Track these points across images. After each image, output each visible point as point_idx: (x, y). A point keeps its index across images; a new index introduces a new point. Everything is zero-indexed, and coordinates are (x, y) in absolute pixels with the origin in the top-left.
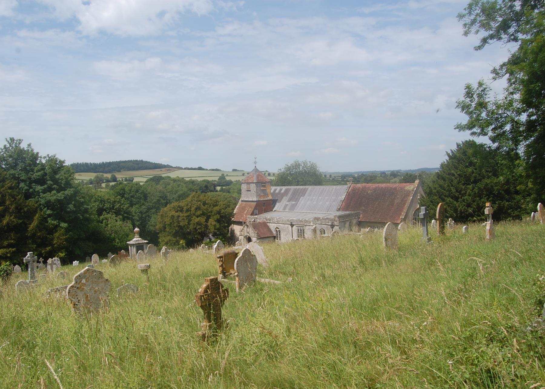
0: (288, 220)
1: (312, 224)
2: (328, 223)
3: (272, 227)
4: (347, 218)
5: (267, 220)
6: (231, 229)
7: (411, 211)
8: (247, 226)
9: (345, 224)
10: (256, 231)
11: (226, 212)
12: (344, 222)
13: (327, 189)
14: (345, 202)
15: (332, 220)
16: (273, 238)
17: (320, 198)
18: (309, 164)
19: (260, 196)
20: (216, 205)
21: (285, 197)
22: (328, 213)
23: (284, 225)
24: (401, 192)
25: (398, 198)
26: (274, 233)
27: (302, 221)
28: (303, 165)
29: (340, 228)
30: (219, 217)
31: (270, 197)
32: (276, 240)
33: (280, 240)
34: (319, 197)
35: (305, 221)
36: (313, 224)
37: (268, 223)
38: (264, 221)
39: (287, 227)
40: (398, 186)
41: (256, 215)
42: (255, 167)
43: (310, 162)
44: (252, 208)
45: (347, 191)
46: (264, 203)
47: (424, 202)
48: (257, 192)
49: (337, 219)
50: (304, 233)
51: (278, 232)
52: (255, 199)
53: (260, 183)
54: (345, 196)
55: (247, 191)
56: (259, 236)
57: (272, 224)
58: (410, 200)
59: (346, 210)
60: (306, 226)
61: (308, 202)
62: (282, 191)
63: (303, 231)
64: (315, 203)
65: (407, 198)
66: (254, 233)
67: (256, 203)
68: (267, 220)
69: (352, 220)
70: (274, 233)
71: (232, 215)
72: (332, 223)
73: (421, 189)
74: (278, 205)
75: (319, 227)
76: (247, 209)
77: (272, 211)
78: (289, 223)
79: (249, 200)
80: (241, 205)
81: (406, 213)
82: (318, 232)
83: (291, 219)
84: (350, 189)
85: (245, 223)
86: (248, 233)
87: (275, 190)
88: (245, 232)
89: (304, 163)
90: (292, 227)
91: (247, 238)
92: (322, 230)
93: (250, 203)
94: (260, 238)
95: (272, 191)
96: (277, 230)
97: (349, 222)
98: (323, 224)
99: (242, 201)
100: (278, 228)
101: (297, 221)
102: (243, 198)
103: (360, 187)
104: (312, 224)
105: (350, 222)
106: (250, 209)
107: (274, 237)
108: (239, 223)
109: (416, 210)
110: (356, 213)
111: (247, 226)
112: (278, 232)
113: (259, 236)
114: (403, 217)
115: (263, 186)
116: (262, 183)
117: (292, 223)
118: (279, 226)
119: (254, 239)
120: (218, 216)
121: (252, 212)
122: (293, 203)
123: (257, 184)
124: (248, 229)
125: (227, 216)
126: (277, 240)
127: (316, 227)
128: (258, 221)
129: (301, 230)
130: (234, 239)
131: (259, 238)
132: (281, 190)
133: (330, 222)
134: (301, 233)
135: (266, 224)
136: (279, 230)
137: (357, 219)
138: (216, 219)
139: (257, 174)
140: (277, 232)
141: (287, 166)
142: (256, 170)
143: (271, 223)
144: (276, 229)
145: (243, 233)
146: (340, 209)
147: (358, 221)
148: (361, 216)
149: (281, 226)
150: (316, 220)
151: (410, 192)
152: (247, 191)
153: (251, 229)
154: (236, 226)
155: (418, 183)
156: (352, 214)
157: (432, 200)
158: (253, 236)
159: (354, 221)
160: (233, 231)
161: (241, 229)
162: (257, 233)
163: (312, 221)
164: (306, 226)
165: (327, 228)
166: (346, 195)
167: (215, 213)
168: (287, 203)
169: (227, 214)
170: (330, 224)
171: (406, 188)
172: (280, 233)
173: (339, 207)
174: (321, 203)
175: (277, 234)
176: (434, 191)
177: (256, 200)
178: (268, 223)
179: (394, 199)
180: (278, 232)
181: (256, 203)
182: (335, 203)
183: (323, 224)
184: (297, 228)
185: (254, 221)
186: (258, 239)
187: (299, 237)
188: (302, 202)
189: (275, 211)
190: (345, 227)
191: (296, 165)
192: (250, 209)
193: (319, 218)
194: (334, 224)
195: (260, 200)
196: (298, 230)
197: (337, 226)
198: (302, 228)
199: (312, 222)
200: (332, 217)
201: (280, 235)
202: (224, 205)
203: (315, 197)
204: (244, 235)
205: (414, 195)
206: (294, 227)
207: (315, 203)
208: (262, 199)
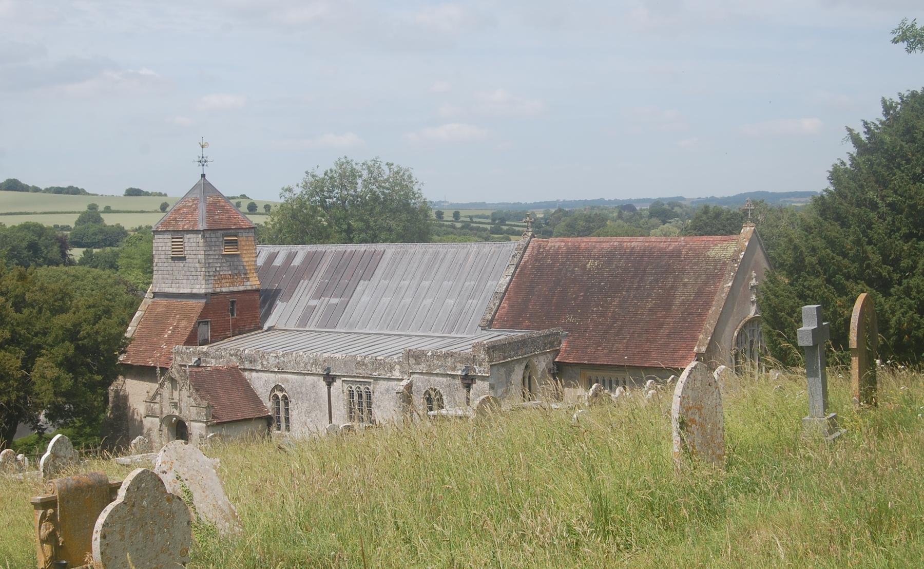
0: (315, 362)
1: (397, 374)
2: (454, 369)
3: (261, 383)
4: (516, 354)
5: (241, 360)
6: (117, 392)
7: (728, 329)
8: (173, 381)
9: (509, 374)
10: (202, 398)
11: (97, 333)
12: (508, 367)
13: (449, 256)
14: (509, 299)
15: (467, 359)
16: (265, 424)
17: (426, 284)
18: (387, 172)
19: (220, 279)
20: (63, 310)
21: (304, 283)
22: (453, 335)
24: (696, 264)
25: (685, 285)
26: (269, 404)
27: (363, 364)
28: (365, 174)
29: (492, 387)
30: (71, 351)
31: (254, 283)
32: (275, 431)
33: (288, 428)
34: (422, 280)
35: (373, 363)
36: (402, 372)
37: (245, 370)
38: (231, 365)
39: (314, 386)
40: (684, 246)
41: (205, 342)
42: (203, 176)
43: (389, 165)
44: (189, 319)
45: (516, 260)
46: (233, 302)
47: (777, 297)
48: (208, 265)
49: (482, 355)
50: (369, 405)
51: (282, 403)
52: (200, 288)
53: (219, 234)
54: (508, 279)
55: (173, 259)
56: (214, 417)
57: (260, 374)
58: (727, 290)
59: (513, 327)
60: (376, 379)
61: (386, 300)
62: (297, 262)
63: (369, 396)
64: (407, 300)
65: (714, 284)
66: (198, 406)
67: (204, 301)
68: (241, 360)
69: (535, 360)
70: (269, 404)
71: (118, 342)
72: (467, 369)
73: (759, 255)
74: (280, 307)
75: (421, 383)
76: (171, 324)
77: (261, 328)
78: (320, 371)
79: (182, 291)
80: (150, 309)
81: (714, 335)
82: (419, 400)
83: (326, 355)
84: (527, 253)
85: (164, 370)
86: (176, 405)
87: (273, 257)
88: (166, 403)
89: (369, 168)
90: (329, 385)
91: (170, 425)
92: (433, 394)
93: (184, 301)
94: (218, 424)
95: (260, 262)
96: (277, 397)
97: (523, 367)
98: (437, 375)
99: (156, 295)
100: (282, 390)
101: (345, 363)
102: (161, 283)
103: (559, 248)
104: (397, 374)
105: (527, 367)
106: (183, 323)
107: (269, 421)
108: (145, 372)
109: (745, 326)
110: (548, 336)
111: (173, 381)
112: (282, 403)
113: (214, 417)
114: (703, 349)
115: (228, 243)
116: (227, 231)
117: (329, 369)
119: (196, 428)
120: (69, 348)
121: (192, 332)
122: (334, 301)
123: (207, 235)
124: (176, 394)
125: (102, 347)
126: (279, 429)
127: (411, 382)
128: (213, 363)
129: (360, 396)
130: (128, 429)
131: (213, 425)
132: (291, 257)
133: (459, 365)
134: (360, 404)
135: (241, 376)
136: (284, 396)
137: (550, 357)
138: (60, 358)
139: (209, 199)
140: (278, 403)
141: (311, 179)
142: (205, 187)
143: (257, 371)
144: (273, 390)
145: (157, 406)
146: (491, 321)
147: (554, 363)
148: (563, 345)
149: (291, 381)
150: (412, 361)
151: (724, 264)
152: (173, 259)
153: (185, 393)
154: (135, 382)
155: (750, 237)
156: (534, 341)
157: (803, 291)
158: (194, 417)
159: (542, 364)
160: (122, 402)
161: (151, 394)
162: (208, 407)
163: (399, 363)
164: (376, 379)
165: (449, 386)
166: (514, 274)
167: (57, 336)
168: (314, 303)
169: (100, 339)
170: (459, 373)
171: (711, 253)
172: (287, 404)
173: (489, 317)
174: (428, 302)
175: (278, 411)
176: (810, 259)
177: (203, 291)
178: (245, 370)
179: (672, 288)
180: (282, 400)
181: (204, 301)
182: (475, 301)
183: (437, 375)
184: (346, 386)
185: (198, 366)
186: (209, 427)
187: (351, 418)
188: (365, 299)
189: (270, 329)
190: (508, 382)
191: (341, 176)
192: (183, 323)
193: (423, 353)
194: (471, 373)
195: (218, 290)
196: (351, 394)
197: (483, 378)
198: (362, 388)
199: (398, 367)
200: (466, 349)
201: (287, 410)
202: (90, 307)
203: (407, 282)
204: (162, 412)
205: (737, 273)
206: (338, 384)
207: (407, 300)
208: (224, 289)
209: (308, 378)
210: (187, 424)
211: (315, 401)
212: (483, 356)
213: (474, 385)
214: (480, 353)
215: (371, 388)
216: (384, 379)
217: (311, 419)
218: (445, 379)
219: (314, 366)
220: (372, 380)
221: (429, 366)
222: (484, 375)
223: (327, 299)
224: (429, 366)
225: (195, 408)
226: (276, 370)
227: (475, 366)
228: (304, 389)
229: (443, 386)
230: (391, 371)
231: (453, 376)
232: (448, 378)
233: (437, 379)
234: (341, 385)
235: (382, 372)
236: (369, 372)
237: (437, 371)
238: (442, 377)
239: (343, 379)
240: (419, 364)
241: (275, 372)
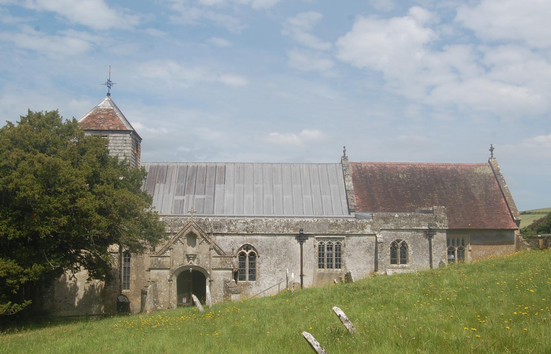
1: (368, 231)
33: (253, 278)
36: (373, 230)
60: (348, 235)
63: (338, 248)
98: (403, 230)
101: (318, 225)
118: (252, 241)
136: (252, 254)
143: (223, 234)
144: (240, 249)
165: (413, 237)
171: (478, 170)
196: (321, 248)
197: (442, 231)
199: (369, 226)
209: (278, 237)
210: (209, 273)
211: (285, 255)
212: (443, 216)
213: (435, 236)
214: (441, 214)
215: (342, 242)
216: (356, 235)
217: (280, 269)
218: (410, 233)
219: (285, 228)
220: (345, 237)
221: (397, 224)
222: (444, 228)
223: (191, 196)
224: (397, 224)
225: (219, 258)
226: (246, 233)
227: (436, 223)
229: (408, 238)
230: (362, 229)
231: (418, 231)
232: (413, 232)
233: (403, 233)
234: (313, 242)
235: (355, 230)
236: (342, 231)
237: (404, 227)
238: (408, 232)
239: (317, 237)
240: (388, 223)
241: (243, 235)
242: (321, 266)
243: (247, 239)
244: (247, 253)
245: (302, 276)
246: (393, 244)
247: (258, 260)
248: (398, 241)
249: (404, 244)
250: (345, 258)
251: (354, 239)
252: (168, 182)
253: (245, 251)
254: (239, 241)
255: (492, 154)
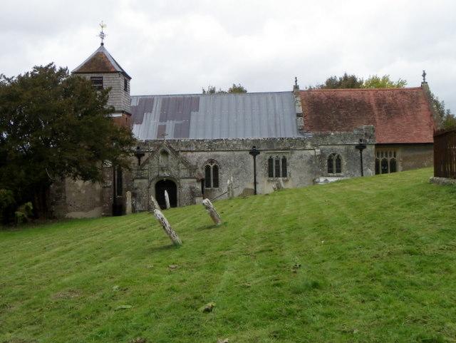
1: (309, 146)
23: (232, 153)
33: (216, 185)
36: (313, 145)
42: (102, 44)
63: (284, 160)
72: (361, 140)
104: (309, 146)
118: (215, 156)
143: (192, 151)
144: (206, 162)
149: (222, 155)
196: (270, 160)
199: (309, 143)
206: (262, 154)
209: (236, 153)
215: (287, 156)
228: (233, 160)
242: (271, 175)
243: (210, 155)
244: (212, 166)
245: (255, 183)
246: (330, 156)
247: (220, 171)
248: (334, 154)
249: (338, 156)
250: (289, 170)
251: (298, 153)
252: (153, 112)
253: (209, 164)
254: (205, 156)
255: (424, 79)
